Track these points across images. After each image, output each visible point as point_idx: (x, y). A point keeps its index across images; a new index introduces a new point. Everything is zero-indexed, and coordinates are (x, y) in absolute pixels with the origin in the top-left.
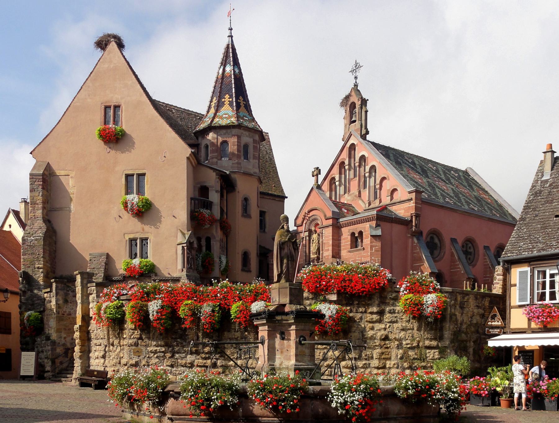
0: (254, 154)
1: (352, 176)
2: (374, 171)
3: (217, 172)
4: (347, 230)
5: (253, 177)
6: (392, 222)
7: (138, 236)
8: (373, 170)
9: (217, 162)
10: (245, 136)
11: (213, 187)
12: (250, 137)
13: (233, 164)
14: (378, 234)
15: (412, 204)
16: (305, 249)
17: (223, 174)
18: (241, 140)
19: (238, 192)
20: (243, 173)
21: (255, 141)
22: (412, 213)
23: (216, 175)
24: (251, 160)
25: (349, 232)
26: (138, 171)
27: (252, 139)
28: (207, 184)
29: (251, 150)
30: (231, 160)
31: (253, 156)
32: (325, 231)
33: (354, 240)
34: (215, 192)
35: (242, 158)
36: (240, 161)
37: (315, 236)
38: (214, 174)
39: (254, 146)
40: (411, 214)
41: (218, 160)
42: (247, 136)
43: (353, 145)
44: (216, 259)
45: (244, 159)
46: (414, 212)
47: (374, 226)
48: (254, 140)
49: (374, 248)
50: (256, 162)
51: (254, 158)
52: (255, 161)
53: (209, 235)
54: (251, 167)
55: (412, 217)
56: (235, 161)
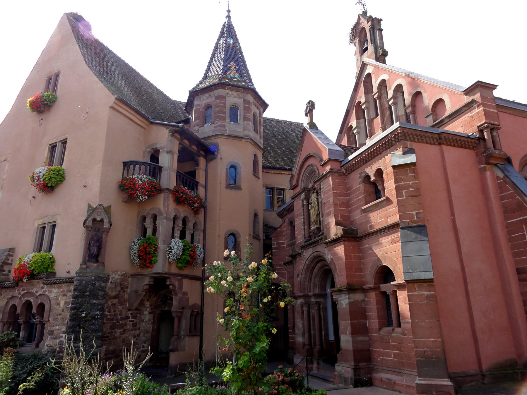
0: (244, 115)
1: (373, 115)
2: (401, 94)
3: (171, 128)
4: (357, 176)
5: (243, 140)
6: (440, 144)
7: (47, 220)
8: (399, 94)
9: (198, 130)
10: (232, 96)
11: (163, 148)
12: (240, 98)
13: (215, 127)
14: (409, 162)
15: (478, 110)
16: (302, 220)
17: (177, 129)
18: (225, 101)
19: (221, 159)
20: (228, 136)
21: (246, 102)
22: (479, 124)
23: (170, 132)
24: (241, 121)
25: (360, 177)
26: (61, 138)
27: (243, 100)
28: (158, 146)
29: (241, 113)
30: (213, 123)
31: (244, 117)
32: (323, 184)
33: (372, 190)
34: (166, 153)
35: (228, 120)
36: (224, 124)
37: (313, 197)
38: (167, 131)
39: (244, 107)
40: (478, 127)
41: (200, 127)
42: (235, 97)
43: (369, 75)
44: (162, 246)
45: (231, 121)
46: (484, 121)
47: (401, 153)
48: (244, 101)
49: (404, 192)
50: (248, 124)
51: (246, 119)
52: (246, 122)
53: (155, 212)
54: (240, 130)
55: (481, 131)
56: (217, 123)
